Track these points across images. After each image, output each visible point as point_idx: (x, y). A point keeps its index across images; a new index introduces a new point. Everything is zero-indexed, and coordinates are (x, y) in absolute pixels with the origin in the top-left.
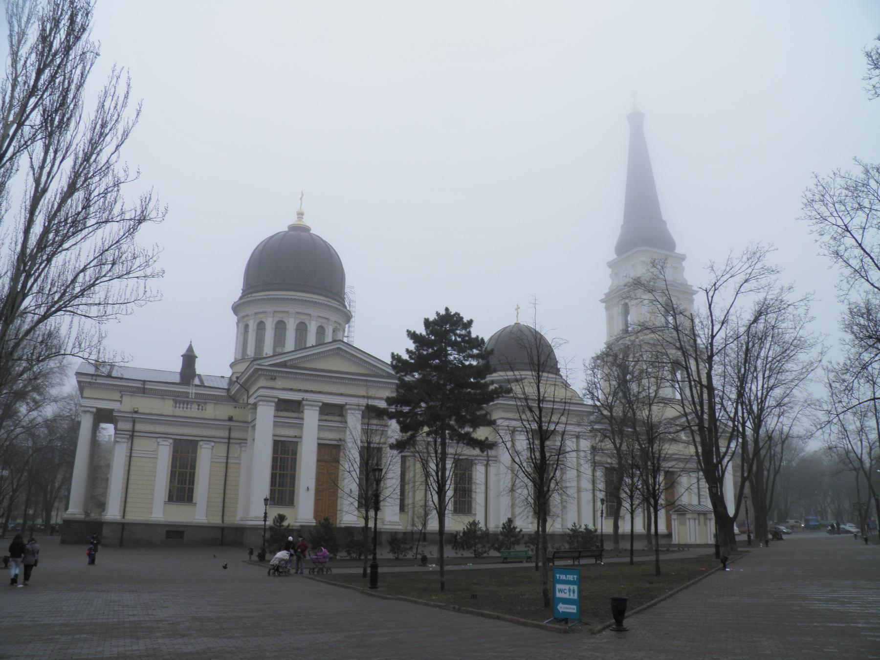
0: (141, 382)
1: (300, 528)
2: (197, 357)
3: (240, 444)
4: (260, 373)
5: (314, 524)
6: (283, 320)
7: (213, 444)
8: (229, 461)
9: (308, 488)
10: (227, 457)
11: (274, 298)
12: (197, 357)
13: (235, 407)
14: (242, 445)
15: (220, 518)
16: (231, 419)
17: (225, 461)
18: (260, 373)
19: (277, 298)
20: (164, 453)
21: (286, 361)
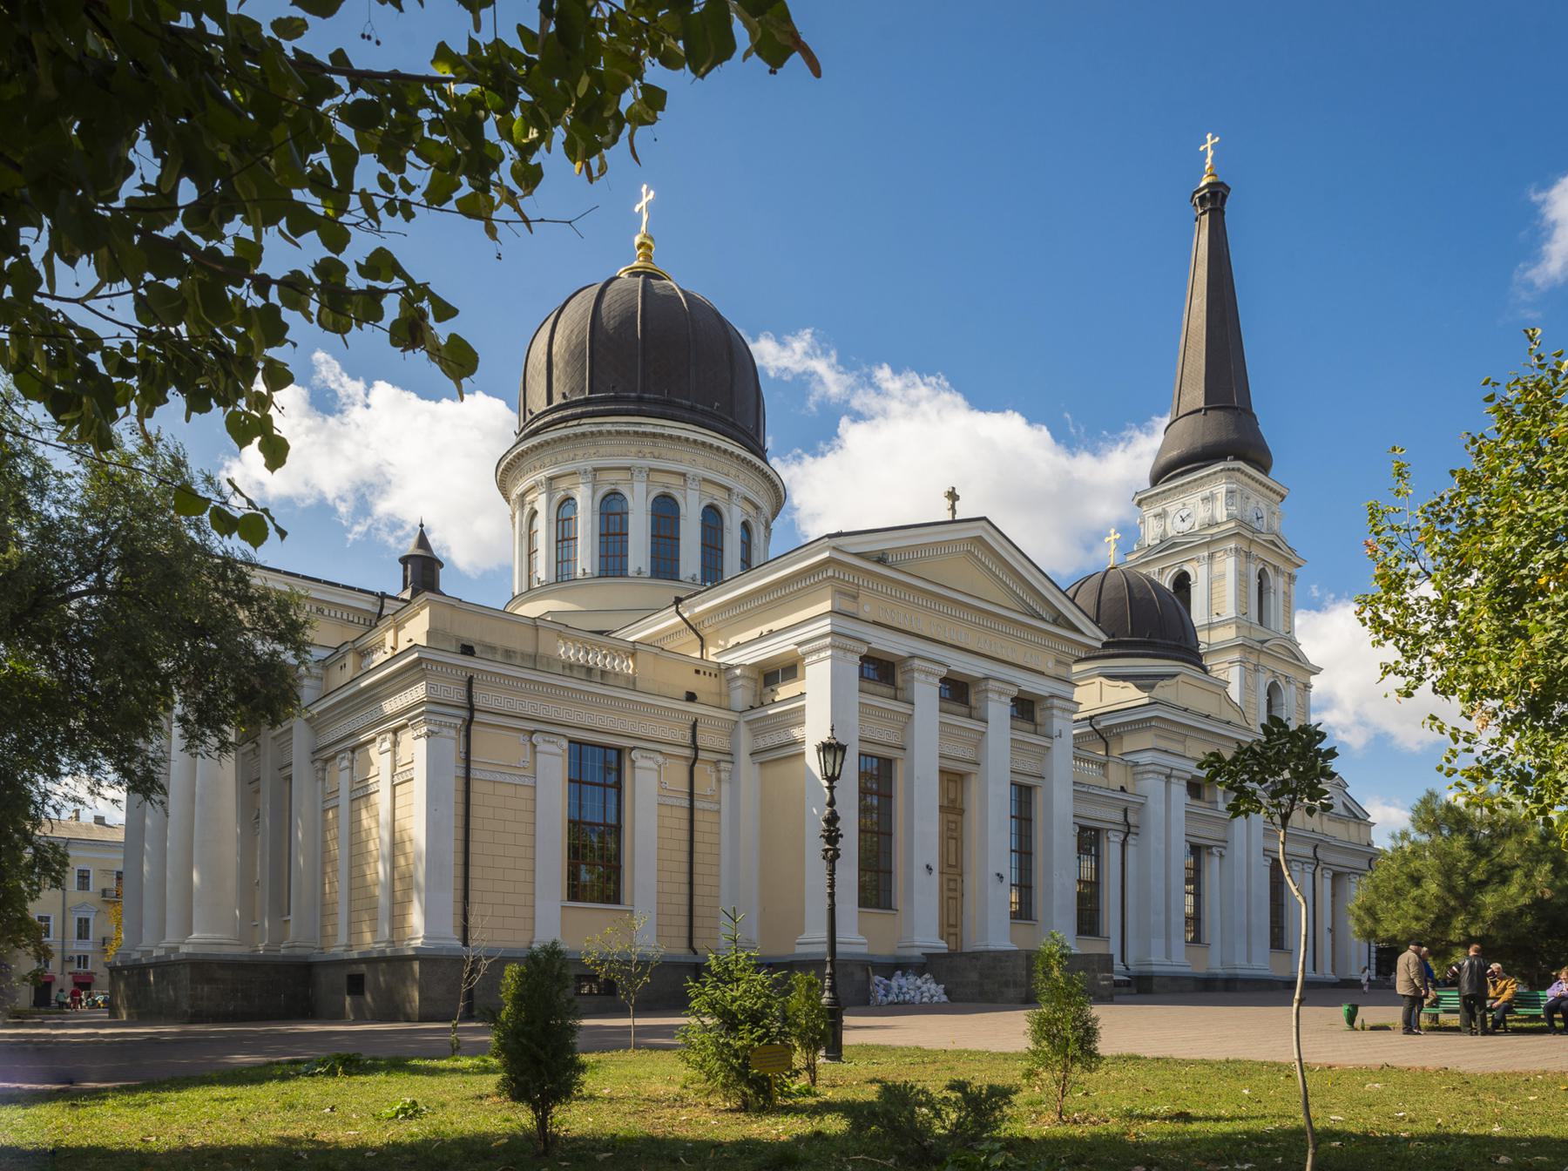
0: (372, 599)
1: (925, 961)
2: (442, 565)
3: (719, 761)
4: (830, 573)
5: (946, 951)
6: (673, 492)
7: (660, 759)
8: (697, 804)
9: (927, 866)
10: (691, 794)
11: (654, 435)
12: (442, 565)
13: (697, 672)
14: (723, 765)
15: (685, 943)
16: (691, 697)
17: (686, 803)
18: (830, 573)
19: (662, 436)
20: (554, 766)
21: (883, 552)
